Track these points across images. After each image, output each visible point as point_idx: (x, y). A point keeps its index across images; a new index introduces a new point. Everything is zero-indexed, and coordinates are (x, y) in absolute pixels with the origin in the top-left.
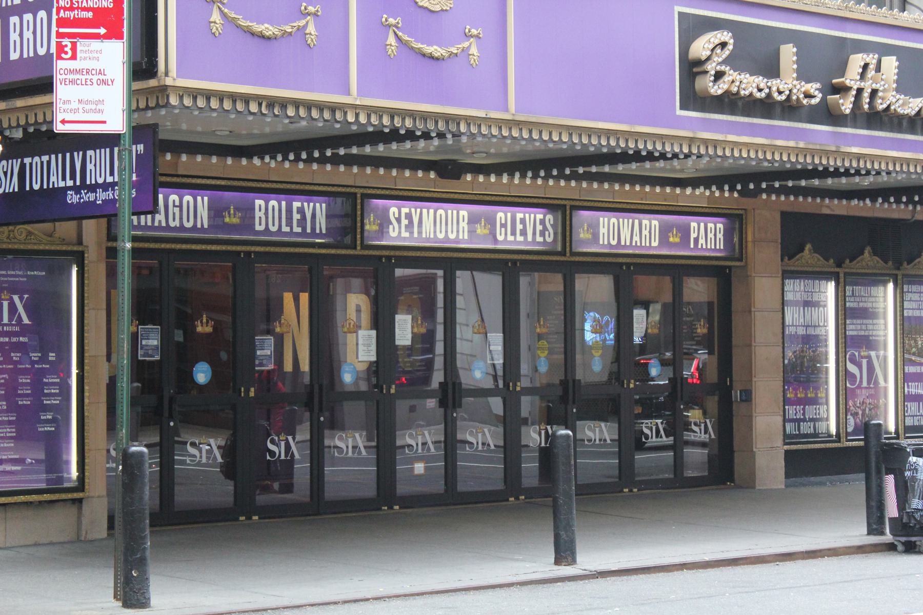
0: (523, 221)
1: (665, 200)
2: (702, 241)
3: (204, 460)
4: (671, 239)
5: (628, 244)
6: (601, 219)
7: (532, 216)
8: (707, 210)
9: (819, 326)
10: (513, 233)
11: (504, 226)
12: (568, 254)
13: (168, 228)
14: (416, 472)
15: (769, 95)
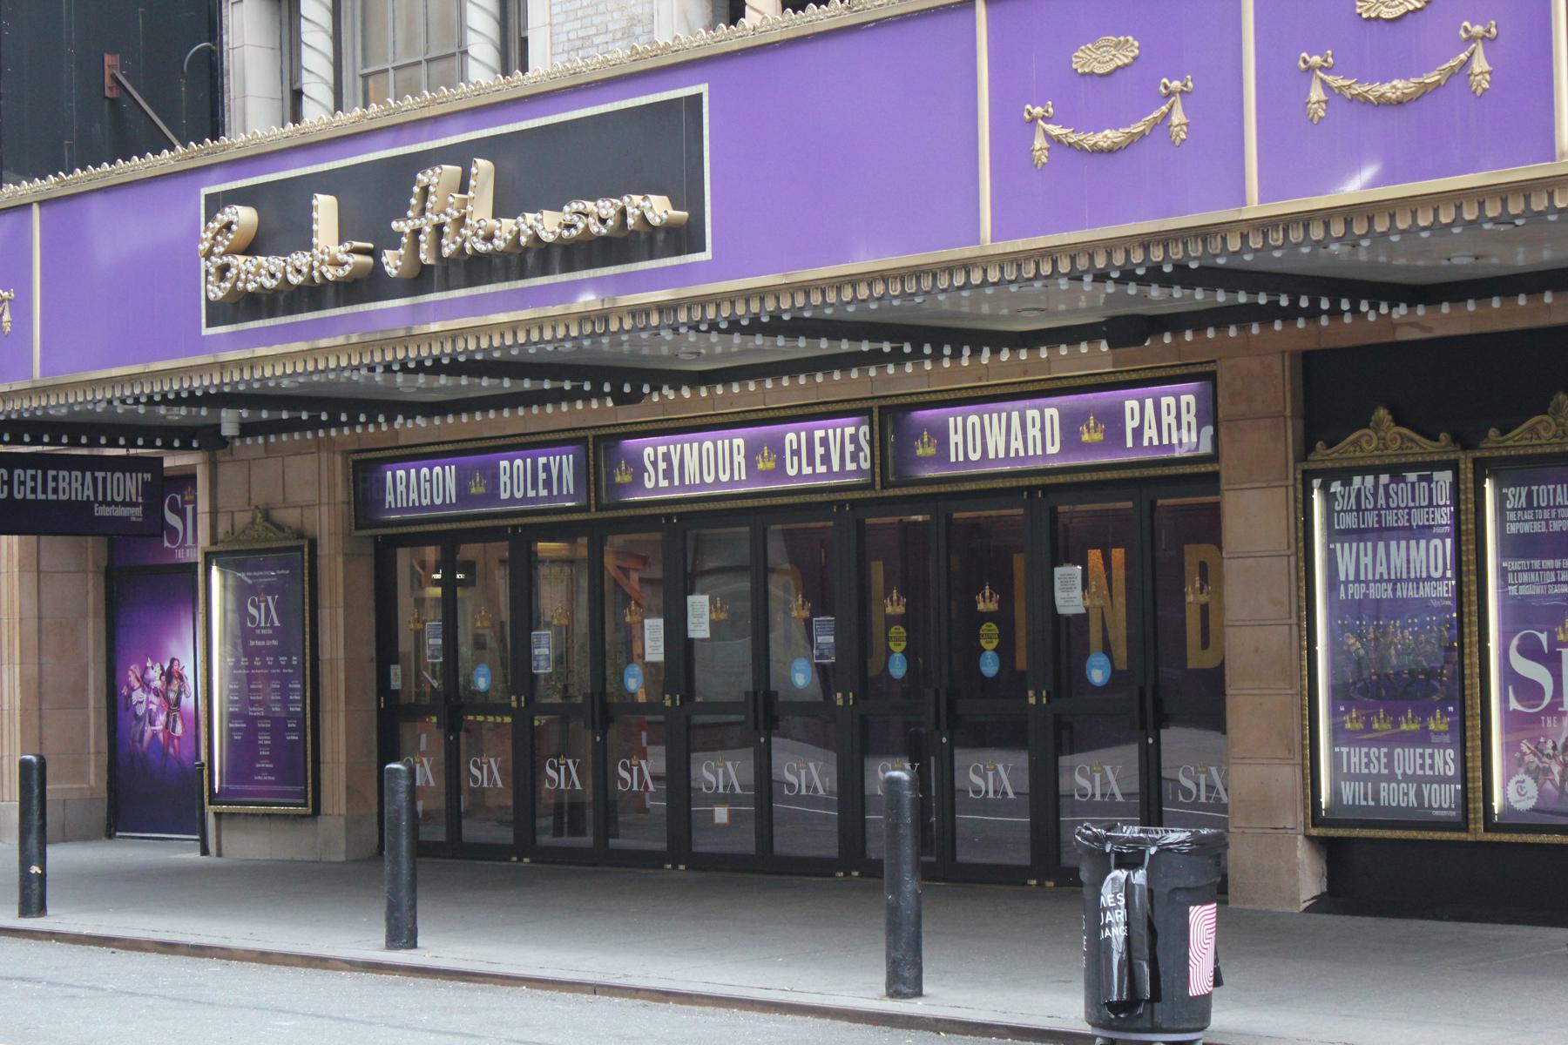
0: (824, 442)
1: (1025, 373)
2: (1150, 433)
3: (1203, 799)
4: (1086, 437)
5: (1002, 455)
6: (951, 420)
7: (839, 431)
8: (1113, 378)
9: (1429, 578)
10: (811, 462)
11: (796, 452)
12: (878, 487)
13: (421, 508)
14: (717, 820)
15: (285, 280)
